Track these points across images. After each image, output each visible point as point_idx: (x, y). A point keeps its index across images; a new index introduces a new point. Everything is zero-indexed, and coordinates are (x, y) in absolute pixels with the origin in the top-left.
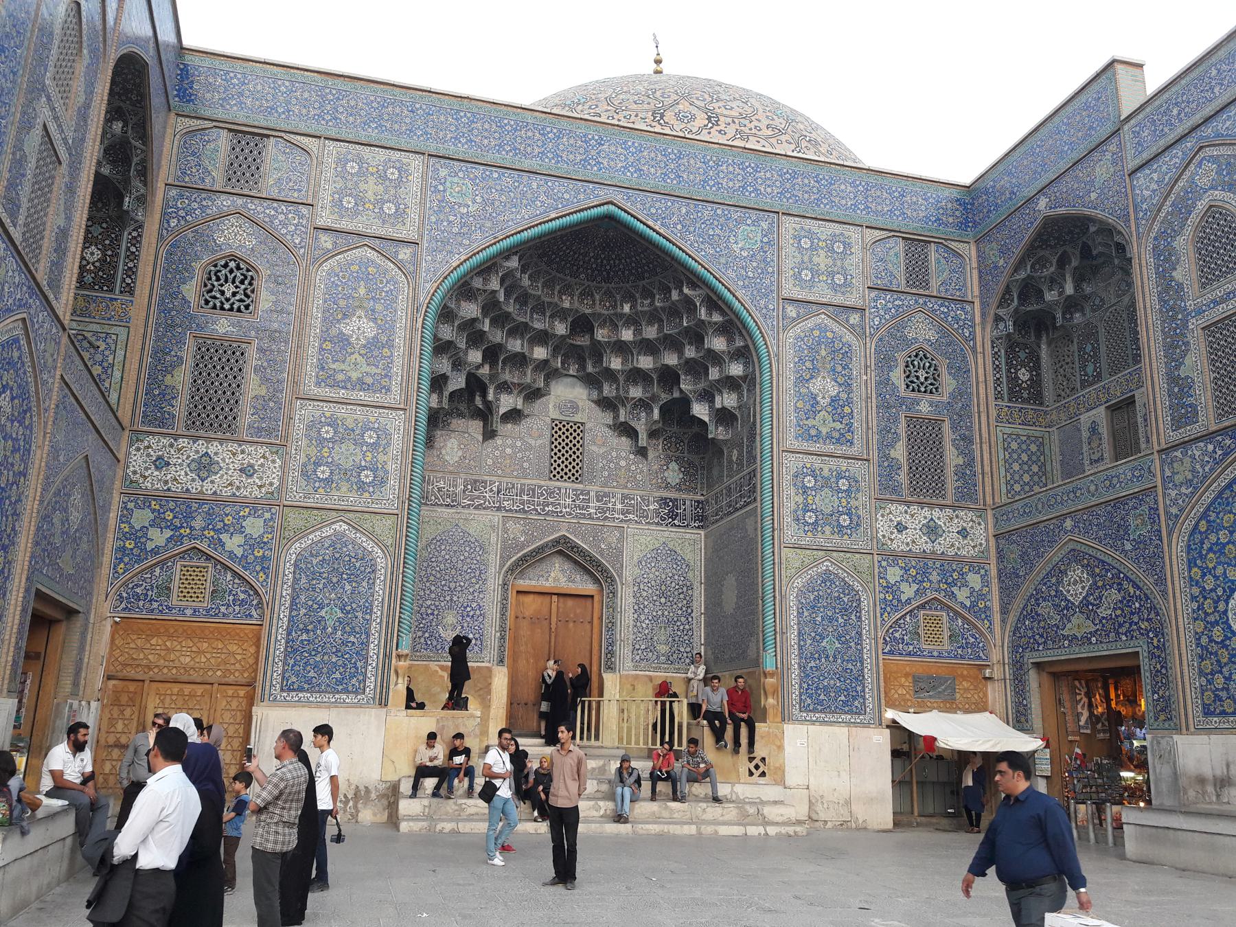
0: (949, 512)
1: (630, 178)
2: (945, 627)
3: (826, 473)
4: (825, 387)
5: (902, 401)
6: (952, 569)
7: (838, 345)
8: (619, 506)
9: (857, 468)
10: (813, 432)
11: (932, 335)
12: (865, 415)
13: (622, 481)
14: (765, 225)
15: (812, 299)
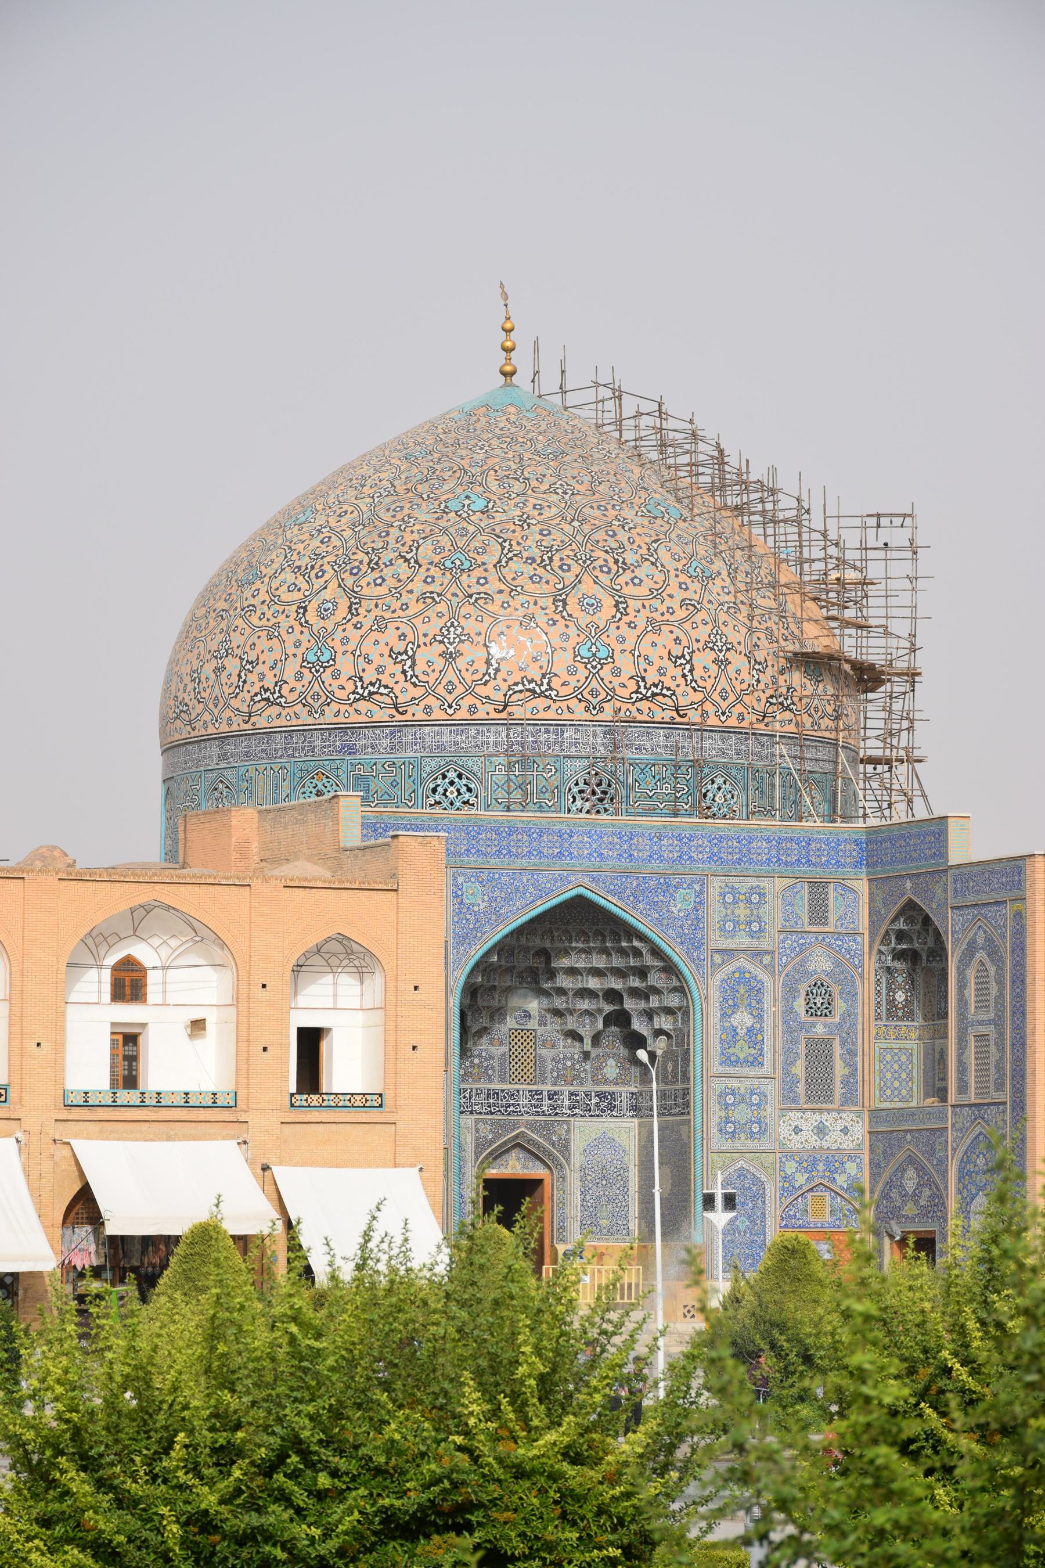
0: (835, 1115)
1: (595, 862)
2: (828, 1203)
3: (742, 1091)
4: (743, 1020)
5: (802, 1026)
6: (834, 1161)
7: (754, 984)
8: (567, 1103)
9: (766, 1086)
10: (733, 1058)
11: (828, 966)
12: (773, 1040)
13: (569, 1079)
14: (697, 887)
15: (734, 946)
